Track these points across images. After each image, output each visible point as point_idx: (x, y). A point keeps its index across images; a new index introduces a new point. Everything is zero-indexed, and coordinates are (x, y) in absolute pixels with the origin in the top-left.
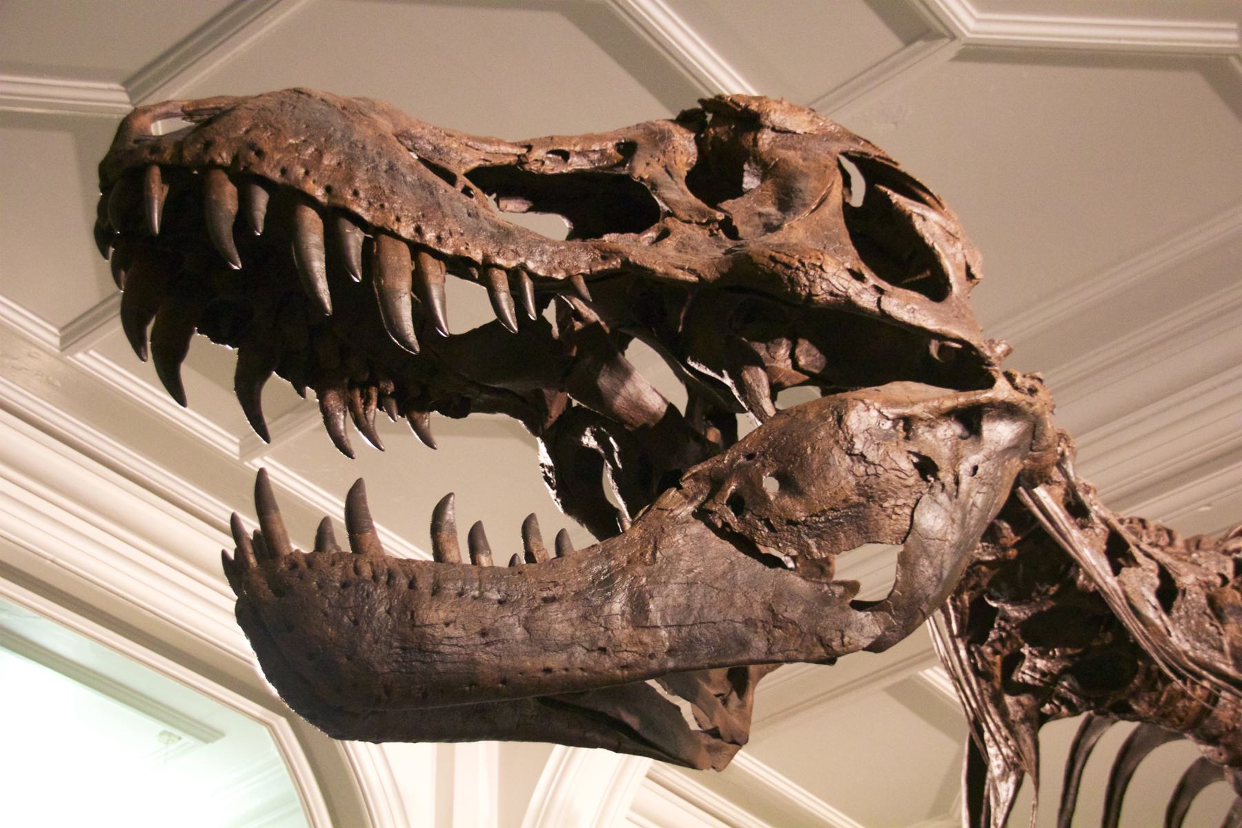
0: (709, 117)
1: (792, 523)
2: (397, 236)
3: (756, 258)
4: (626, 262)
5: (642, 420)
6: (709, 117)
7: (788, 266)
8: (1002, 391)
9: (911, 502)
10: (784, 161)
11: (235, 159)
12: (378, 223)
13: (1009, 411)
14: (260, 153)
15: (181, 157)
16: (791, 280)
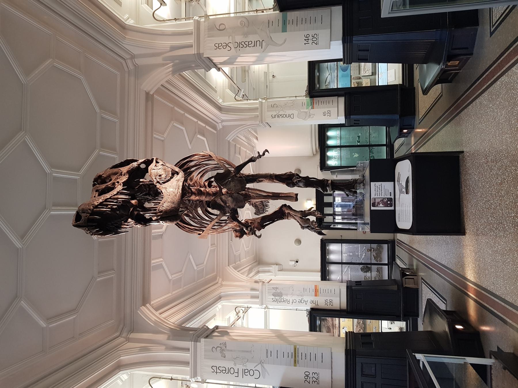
0: (95, 183)
1: (166, 176)
2: (111, 197)
3: (128, 170)
4: (122, 183)
5: (137, 203)
6: (95, 183)
7: (131, 167)
8: (155, 158)
9: (167, 167)
10: (109, 174)
11: (93, 207)
12: (109, 197)
13: (157, 159)
14: (94, 204)
15: (90, 213)
16: (133, 167)
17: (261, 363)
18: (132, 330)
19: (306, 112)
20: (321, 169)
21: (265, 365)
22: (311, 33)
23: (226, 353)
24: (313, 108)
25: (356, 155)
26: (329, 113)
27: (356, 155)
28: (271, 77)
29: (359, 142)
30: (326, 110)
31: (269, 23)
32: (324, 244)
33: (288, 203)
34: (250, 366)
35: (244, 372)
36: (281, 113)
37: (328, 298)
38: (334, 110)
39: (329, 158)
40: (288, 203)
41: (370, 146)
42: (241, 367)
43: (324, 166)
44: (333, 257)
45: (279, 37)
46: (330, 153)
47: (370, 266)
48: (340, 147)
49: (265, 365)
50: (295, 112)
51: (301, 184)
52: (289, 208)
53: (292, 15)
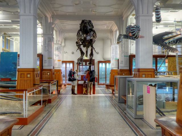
17: (48, 50)
18: (52, 18)
19: (114, 58)
20: (98, 61)
21: (47, 51)
22: (123, 63)
23: (49, 42)
24: (115, 60)
25: (103, 73)
26: (113, 65)
27: (103, 73)
28: (132, 44)
29: (107, 74)
30: (114, 64)
31: (127, 52)
32: (73, 62)
33: (85, 55)
34: (47, 48)
35: (45, 47)
36: (114, 50)
37: (57, 64)
38: (114, 66)
39: (102, 64)
40: (85, 55)
41: (106, 77)
42: (46, 46)
43: (99, 62)
44: (68, 65)
45: (123, 55)
46: (104, 64)
47: (65, 77)
48: (106, 68)
49: (47, 51)
50: (114, 55)
51: (90, 58)
52: (84, 55)
53: (128, 58)
